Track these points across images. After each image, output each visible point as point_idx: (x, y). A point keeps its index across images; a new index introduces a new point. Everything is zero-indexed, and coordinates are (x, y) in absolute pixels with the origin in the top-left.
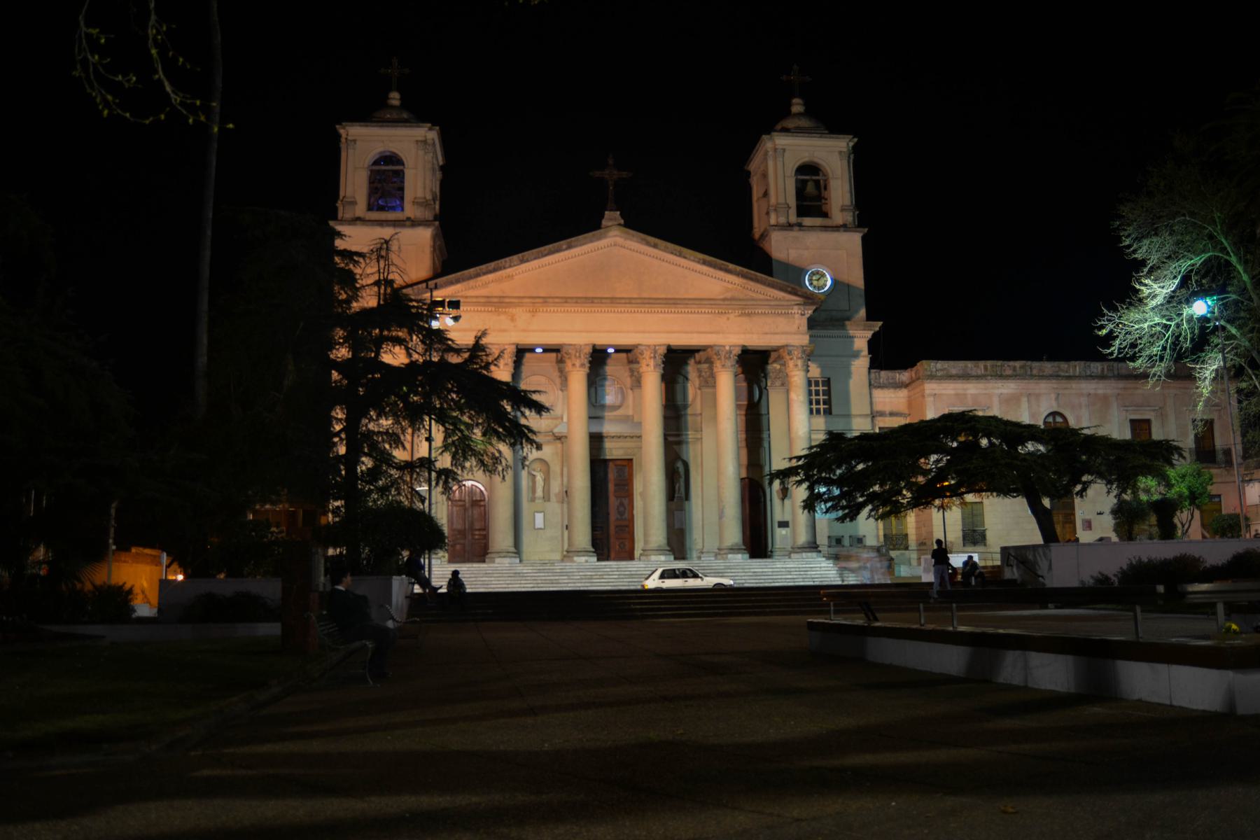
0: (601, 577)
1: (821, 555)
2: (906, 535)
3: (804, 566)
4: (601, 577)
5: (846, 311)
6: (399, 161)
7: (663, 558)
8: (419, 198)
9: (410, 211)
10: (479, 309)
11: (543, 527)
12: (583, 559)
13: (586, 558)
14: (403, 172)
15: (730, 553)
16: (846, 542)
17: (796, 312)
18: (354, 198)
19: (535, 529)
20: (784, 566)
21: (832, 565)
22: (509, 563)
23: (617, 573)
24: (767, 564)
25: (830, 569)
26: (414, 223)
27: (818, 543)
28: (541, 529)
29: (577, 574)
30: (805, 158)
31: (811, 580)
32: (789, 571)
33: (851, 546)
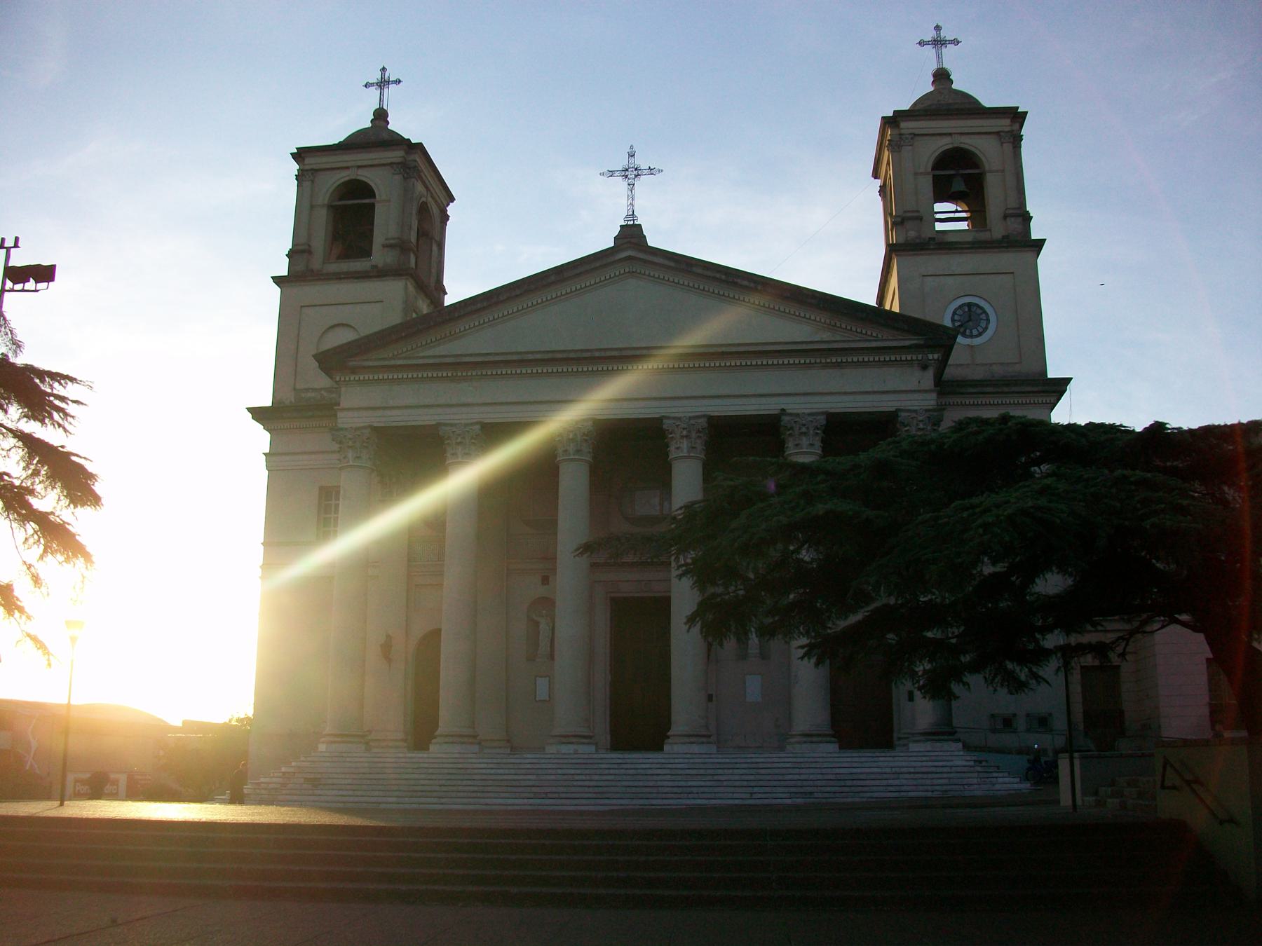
0: (588, 777)
1: (960, 745)
2: (1122, 713)
3: (924, 764)
4: (588, 777)
5: (1016, 363)
6: (371, 194)
7: (696, 749)
8: (394, 239)
9: (380, 257)
10: (430, 375)
11: (548, 699)
12: (565, 749)
13: (576, 747)
14: (372, 206)
15: (805, 742)
16: (1021, 724)
17: (914, 358)
18: (309, 246)
19: (536, 701)
20: (891, 764)
21: (972, 763)
22: (460, 753)
23: (617, 772)
24: (863, 759)
25: (965, 769)
26: (380, 273)
27: (954, 724)
28: (545, 701)
29: (553, 772)
30: (944, 144)
31: (929, 788)
32: (896, 773)
33: (1028, 731)
